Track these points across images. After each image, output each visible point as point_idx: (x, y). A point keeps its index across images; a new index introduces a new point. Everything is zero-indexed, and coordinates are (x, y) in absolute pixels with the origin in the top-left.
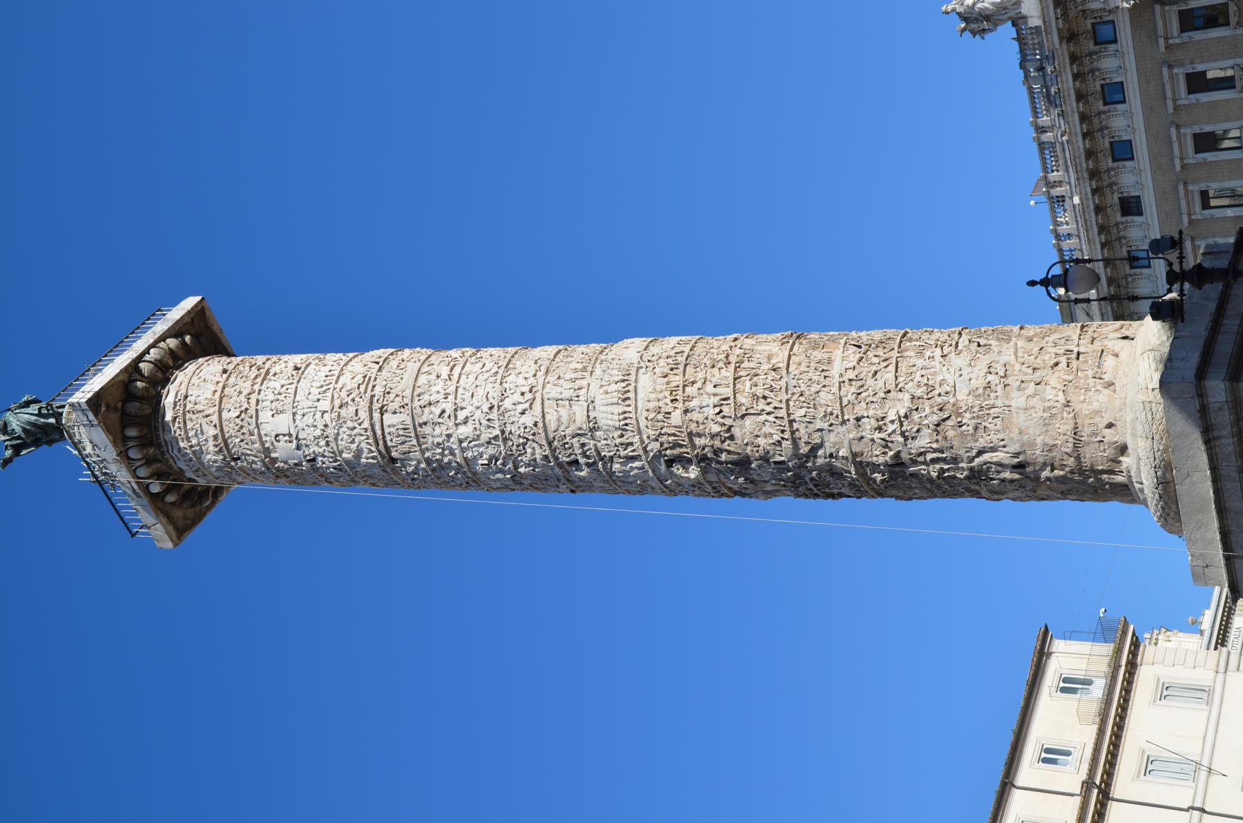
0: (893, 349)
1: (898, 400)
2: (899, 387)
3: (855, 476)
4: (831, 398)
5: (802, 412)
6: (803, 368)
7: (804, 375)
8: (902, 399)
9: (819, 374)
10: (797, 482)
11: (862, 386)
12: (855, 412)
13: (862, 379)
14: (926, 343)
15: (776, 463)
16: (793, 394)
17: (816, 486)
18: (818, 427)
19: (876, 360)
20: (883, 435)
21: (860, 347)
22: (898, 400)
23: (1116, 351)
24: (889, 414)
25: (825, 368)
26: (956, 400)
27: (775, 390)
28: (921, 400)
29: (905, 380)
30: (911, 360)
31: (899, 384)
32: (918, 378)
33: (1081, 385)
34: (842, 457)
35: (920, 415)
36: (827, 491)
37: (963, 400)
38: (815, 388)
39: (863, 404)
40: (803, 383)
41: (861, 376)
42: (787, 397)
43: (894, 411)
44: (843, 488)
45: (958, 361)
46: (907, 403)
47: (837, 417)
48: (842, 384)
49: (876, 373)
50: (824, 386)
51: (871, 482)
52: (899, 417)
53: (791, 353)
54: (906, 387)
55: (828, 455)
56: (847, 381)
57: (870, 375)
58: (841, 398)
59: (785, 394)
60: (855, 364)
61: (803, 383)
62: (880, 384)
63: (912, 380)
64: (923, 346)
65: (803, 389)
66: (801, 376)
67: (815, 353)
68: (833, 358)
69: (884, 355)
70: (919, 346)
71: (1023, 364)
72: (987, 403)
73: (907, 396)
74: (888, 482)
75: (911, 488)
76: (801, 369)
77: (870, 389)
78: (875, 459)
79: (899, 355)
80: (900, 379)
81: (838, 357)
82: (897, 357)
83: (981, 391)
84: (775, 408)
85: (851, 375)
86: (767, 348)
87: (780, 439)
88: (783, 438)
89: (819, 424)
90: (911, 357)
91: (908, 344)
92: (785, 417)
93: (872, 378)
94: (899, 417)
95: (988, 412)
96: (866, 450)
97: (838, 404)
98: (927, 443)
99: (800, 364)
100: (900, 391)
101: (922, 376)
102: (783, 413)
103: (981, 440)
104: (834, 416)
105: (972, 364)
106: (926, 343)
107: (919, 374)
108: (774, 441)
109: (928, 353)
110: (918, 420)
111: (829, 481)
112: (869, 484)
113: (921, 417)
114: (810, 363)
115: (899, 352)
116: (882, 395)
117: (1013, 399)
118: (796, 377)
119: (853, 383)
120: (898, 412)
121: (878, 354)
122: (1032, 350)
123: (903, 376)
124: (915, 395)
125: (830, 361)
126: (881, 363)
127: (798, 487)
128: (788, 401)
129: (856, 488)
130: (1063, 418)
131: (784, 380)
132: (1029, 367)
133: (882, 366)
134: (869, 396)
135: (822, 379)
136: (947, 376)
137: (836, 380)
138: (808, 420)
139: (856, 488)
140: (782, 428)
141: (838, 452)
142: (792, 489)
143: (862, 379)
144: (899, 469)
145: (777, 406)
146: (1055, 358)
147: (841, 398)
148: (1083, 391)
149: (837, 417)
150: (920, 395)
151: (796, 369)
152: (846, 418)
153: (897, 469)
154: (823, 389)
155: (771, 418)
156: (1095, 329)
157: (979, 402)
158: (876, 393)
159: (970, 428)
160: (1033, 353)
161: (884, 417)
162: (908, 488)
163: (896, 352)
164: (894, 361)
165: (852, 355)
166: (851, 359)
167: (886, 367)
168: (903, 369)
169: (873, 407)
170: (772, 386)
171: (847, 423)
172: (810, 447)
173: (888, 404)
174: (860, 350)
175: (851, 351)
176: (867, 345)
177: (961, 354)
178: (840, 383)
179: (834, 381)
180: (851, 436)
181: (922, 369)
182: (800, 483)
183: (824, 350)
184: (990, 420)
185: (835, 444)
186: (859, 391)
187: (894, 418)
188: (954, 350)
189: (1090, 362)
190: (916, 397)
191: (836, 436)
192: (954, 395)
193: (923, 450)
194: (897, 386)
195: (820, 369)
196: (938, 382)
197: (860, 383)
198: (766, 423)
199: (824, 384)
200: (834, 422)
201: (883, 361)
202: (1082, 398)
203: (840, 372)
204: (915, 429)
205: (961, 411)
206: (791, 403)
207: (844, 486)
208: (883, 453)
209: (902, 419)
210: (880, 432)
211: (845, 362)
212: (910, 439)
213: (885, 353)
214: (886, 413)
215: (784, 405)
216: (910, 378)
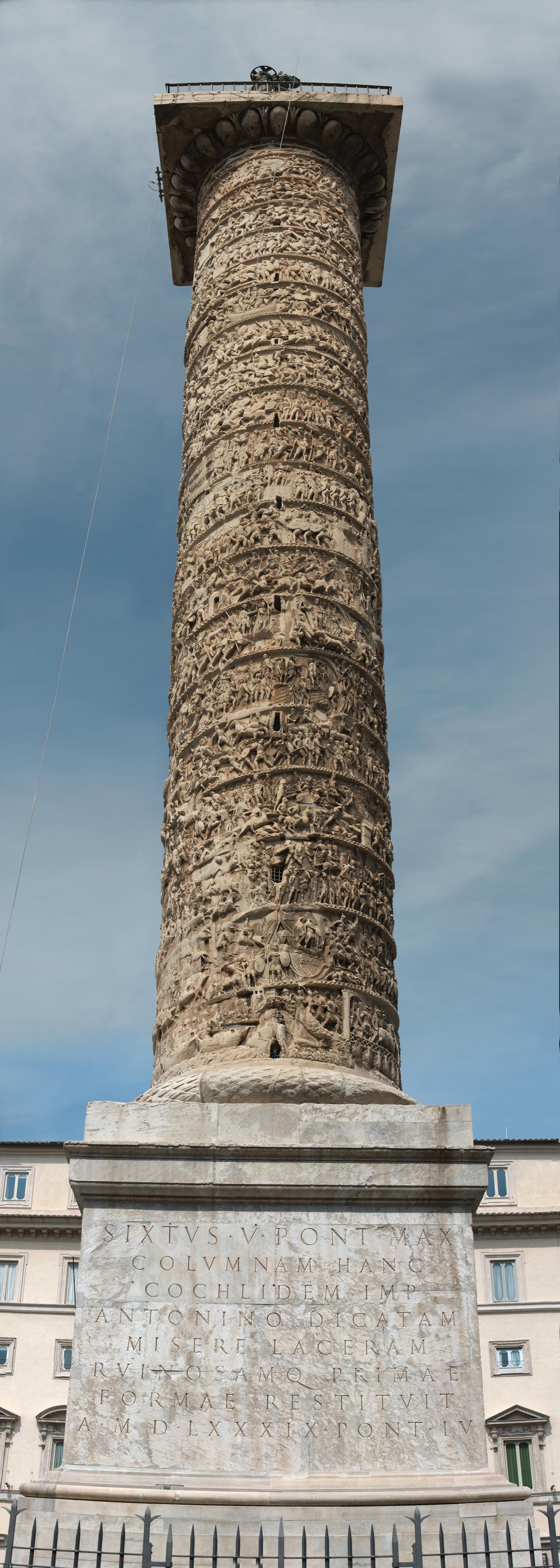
23: (249, 1041)
37: (191, 881)
45: (244, 851)
71: (232, 931)
79: (256, 776)
82: (251, 777)
101: (219, 818)
106: (280, 802)
115: (262, 776)
132: (225, 938)
136: (217, 847)
148: (194, 1018)
156: (310, 1004)
157: (187, 900)
175: (264, 719)
188: (260, 838)
196: (211, 839)
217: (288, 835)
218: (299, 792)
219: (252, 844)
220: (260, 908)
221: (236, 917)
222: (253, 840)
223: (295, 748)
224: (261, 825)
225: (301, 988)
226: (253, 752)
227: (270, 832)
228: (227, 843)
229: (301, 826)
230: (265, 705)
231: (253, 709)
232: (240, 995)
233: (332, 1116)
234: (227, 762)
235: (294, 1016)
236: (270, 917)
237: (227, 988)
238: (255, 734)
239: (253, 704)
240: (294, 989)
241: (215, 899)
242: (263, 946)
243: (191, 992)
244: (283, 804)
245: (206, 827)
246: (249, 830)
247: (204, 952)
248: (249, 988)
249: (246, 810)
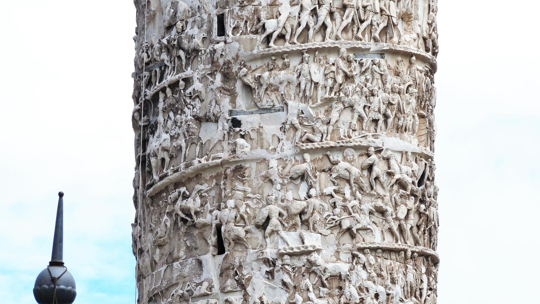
0: (417, 243)
1: (338, 252)
2: (361, 255)
3: (196, 162)
4: (341, 131)
5: (318, 77)
6: (391, 79)
7: (380, 81)
8: (338, 259)
9: (382, 110)
10: (182, 53)
11: (361, 189)
12: (318, 174)
13: (372, 188)
15: (221, 19)
16: (349, 62)
17: (174, 86)
18: (290, 103)
19: (402, 212)
20: (274, 221)
21: (420, 183)
22: (338, 252)
24: (313, 234)
25: (390, 121)
27: (355, 29)
28: (336, 291)
30: (401, 275)
31: (364, 254)
32: (374, 288)
34: (235, 144)
35: (311, 289)
36: (161, 105)
38: (360, 102)
39: (330, 189)
40: (367, 80)
41: (378, 189)
42: (343, 49)
43: (318, 246)
44: (167, 136)
46: (333, 267)
47: (309, 140)
48: (364, 152)
49: (382, 212)
50: (361, 119)
51: (183, 189)
52: (309, 253)
53: (414, 58)
54: (359, 267)
55: (238, 117)
56: (368, 161)
57: (379, 203)
58: (342, 149)
59: (349, 46)
60: (397, 176)
61: (367, 80)
62: (365, 220)
63: (370, 278)
64: (421, 295)
65: (357, 80)
66: (377, 76)
67: (413, 101)
68: (406, 134)
69: (409, 226)
73: (344, 268)
74: (184, 221)
75: (171, 259)
76: (389, 78)
77: (356, 203)
78: (231, 203)
79: (409, 254)
80: (372, 259)
81: (407, 144)
82: (405, 251)
84: (324, 26)
85: (379, 169)
86: (420, 12)
87: (269, 31)
88: (268, 38)
89: (295, 105)
90: (405, 275)
91: (424, 270)
92: (309, 45)
93: (375, 207)
94: (309, 253)
96: (249, 190)
97: (332, 144)
98: (261, 298)
99: (397, 74)
100: (354, 256)
102: (316, 42)
104: (311, 136)
107: (381, 289)
108: (263, 20)
110: (303, 285)
111: (183, 112)
112: (177, 184)
113: (308, 290)
114: (399, 93)
116: (346, 224)
118: (376, 68)
119: (366, 173)
120: (318, 251)
121: (412, 216)
123: (377, 261)
124: (347, 283)
125: (400, 129)
126: (397, 223)
127: (169, 52)
128: (336, 50)
129: (167, 159)
131: (373, 47)
133: (392, 223)
134: (345, 200)
135: (374, 115)
137: (370, 141)
138: (303, 87)
139: (167, 159)
140: (288, 37)
141: (242, 137)
142: (165, 41)
143: (372, 188)
144: (209, 241)
145: (329, 30)
147: (342, 149)
149: (309, 140)
150: (347, 291)
151: (389, 67)
152: (307, 156)
153: (213, 239)
154: (356, 116)
155: (306, 18)
158: (350, 214)
161: (308, 226)
162: (171, 254)
163: (414, 249)
164: (400, 245)
165: (410, 170)
166: (405, 168)
167: (390, 230)
168: (388, 262)
169: (326, 206)
170: (362, 22)
171: (298, 158)
172: (253, 85)
173: (332, 237)
174: (416, 182)
175: (415, 167)
176: (423, 195)
178: (367, 148)
179: (371, 139)
180: (274, 163)
181: (388, 295)
182: (179, 57)
183: (417, 118)
185: (259, 132)
186: (352, 181)
187: (307, 243)
190: (342, 284)
191: (274, 135)
193: (249, 289)
194: (361, 250)
195: (389, 112)
197: (366, 185)
198: (298, 8)
199: (366, 119)
200: (299, 134)
201: (400, 226)
203: (384, 148)
204: (287, 279)
206: (332, 59)
207: (172, 138)
208: (242, 218)
209: (304, 258)
210: (280, 214)
211: (398, 157)
212: (268, 269)
213: (411, 228)
214: (314, 229)
215: (329, 42)
216: (374, 274)
234: (382, 212)
238: (410, 187)
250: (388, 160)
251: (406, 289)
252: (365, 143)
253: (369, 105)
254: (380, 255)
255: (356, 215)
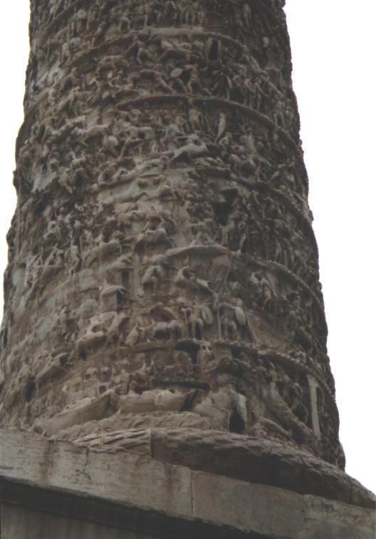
14: (223, 135)
26: (96, 193)
29: (134, 116)
31: (128, 111)
33: (117, 363)
39: (94, 80)
49: (151, 77)
70: (216, 129)
72: (88, 234)
80: (137, 112)
82: (185, 101)
83: (109, 219)
90: (187, 117)
95: (72, 241)
103: (35, 257)
105: (170, 198)
106: (223, 135)
109: (194, 136)
116: (106, 94)
117: (94, 269)
120: (80, 125)
122: (205, 278)
126: (172, 83)
130: (54, 355)
136: (139, 167)
146: (182, 313)
148: (106, 369)
154: (120, 24)
156: (275, 379)
159: (50, 231)
160: (193, 277)
164: (174, 93)
177: (192, 180)
184: (60, 252)
189: (172, 367)
192: (103, 188)
196: (129, 158)
202: (91, 371)
205: (76, 206)
217: (233, 175)
218: (243, 133)
219: (190, 173)
220: (207, 246)
221: (169, 252)
222: (192, 169)
223: (234, 84)
224: (202, 154)
225: (262, 357)
226: (186, 76)
227: (212, 163)
228: (154, 165)
229: (248, 171)
230: (199, 29)
231: (182, 30)
232: (181, 347)
233: (350, 520)
235: (255, 389)
236: (220, 261)
237: (161, 334)
238: (188, 56)
239: (184, 25)
240: (253, 355)
241: (136, 227)
242: (211, 294)
243: (100, 334)
244: (226, 138)
245: (122, 143)
246: (185, 159)
247: (119, 287)
248: (195, 340)
249: (180, 135)
250: (158, 43)
251: (188, 127)
252: (126, 36)
253: (133, 13)
254: (148, 107)
255: (117, 86)
